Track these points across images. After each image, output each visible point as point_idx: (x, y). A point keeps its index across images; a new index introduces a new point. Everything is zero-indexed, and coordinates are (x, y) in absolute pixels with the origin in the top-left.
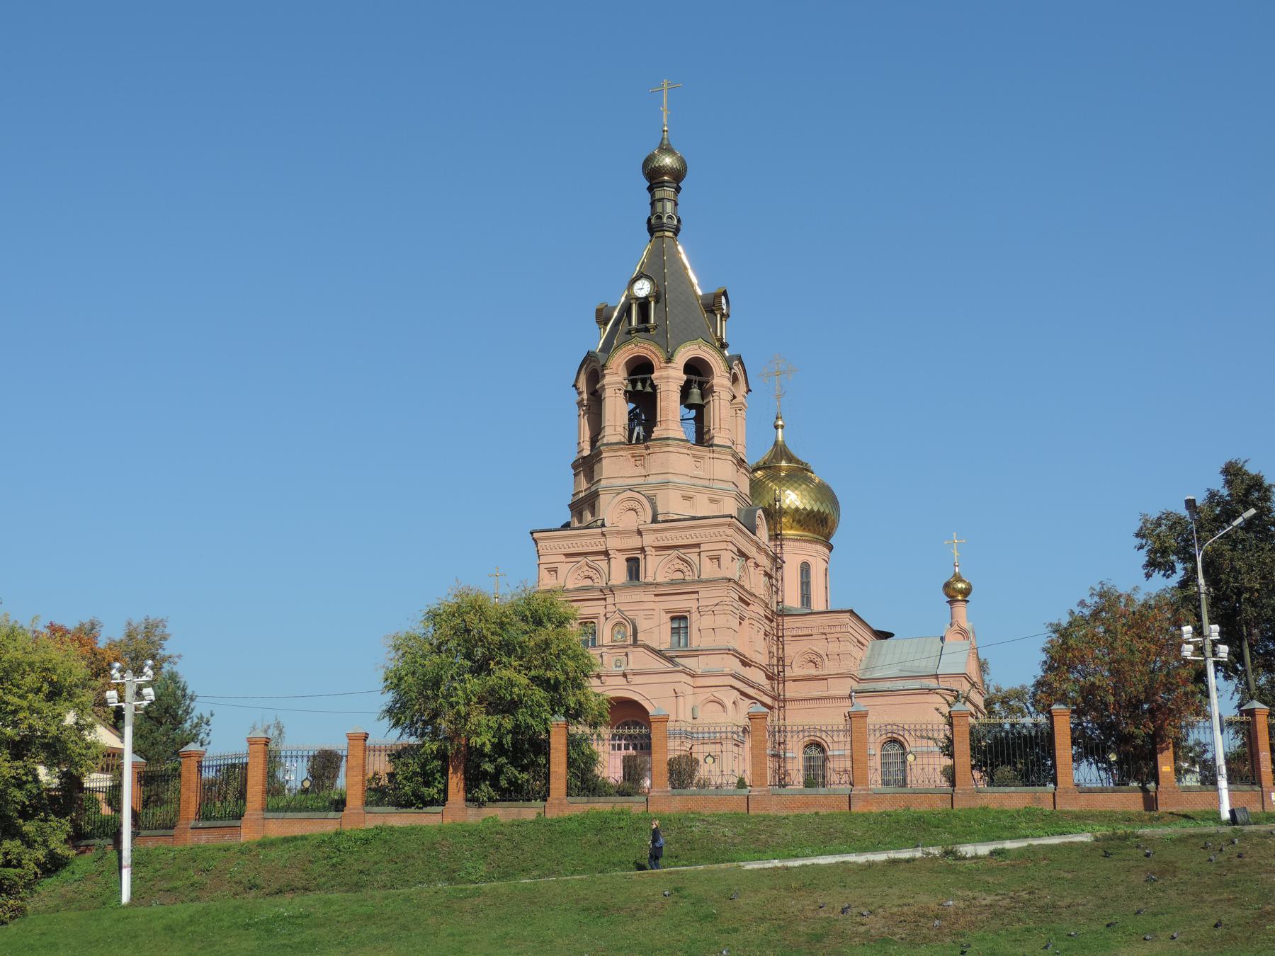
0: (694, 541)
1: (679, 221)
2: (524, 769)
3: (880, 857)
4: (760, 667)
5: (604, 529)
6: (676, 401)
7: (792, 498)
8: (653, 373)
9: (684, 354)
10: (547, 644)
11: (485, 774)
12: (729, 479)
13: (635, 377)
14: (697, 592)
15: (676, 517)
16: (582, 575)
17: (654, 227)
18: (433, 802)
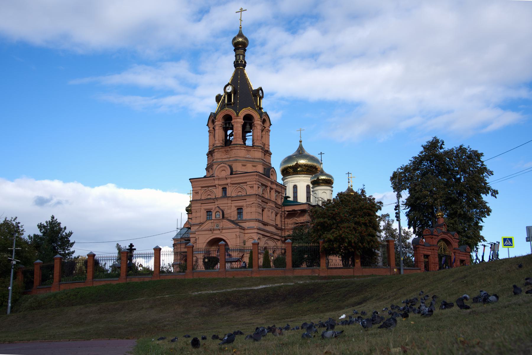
4: (272, 226)
5: (214, 178)
6: (240, 131)
8: (232, 120)
12: (260, 158)
13: (226, 122)
14: (246, 199)
15: (239, 172)
16: (206, 195)
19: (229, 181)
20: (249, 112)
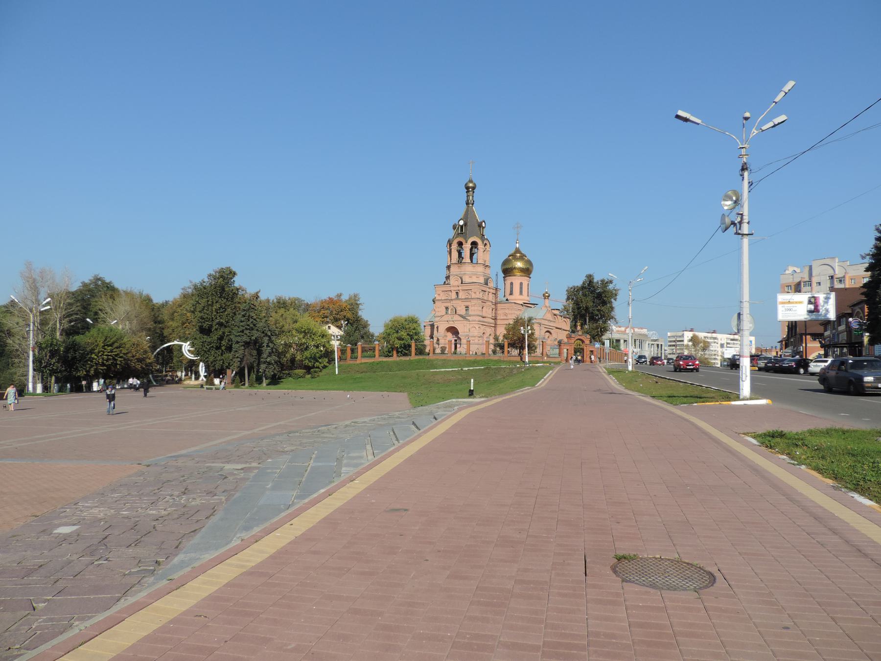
1: (473, 201)
2: (407, 350)
3: (451, 370)
7: (519, 264)
8: (463, 245)
9: (470, 241)
10: (410, 328)
11: (400, 352)
17: (467, 204)
18: (391, 356)
19: (460, 288)
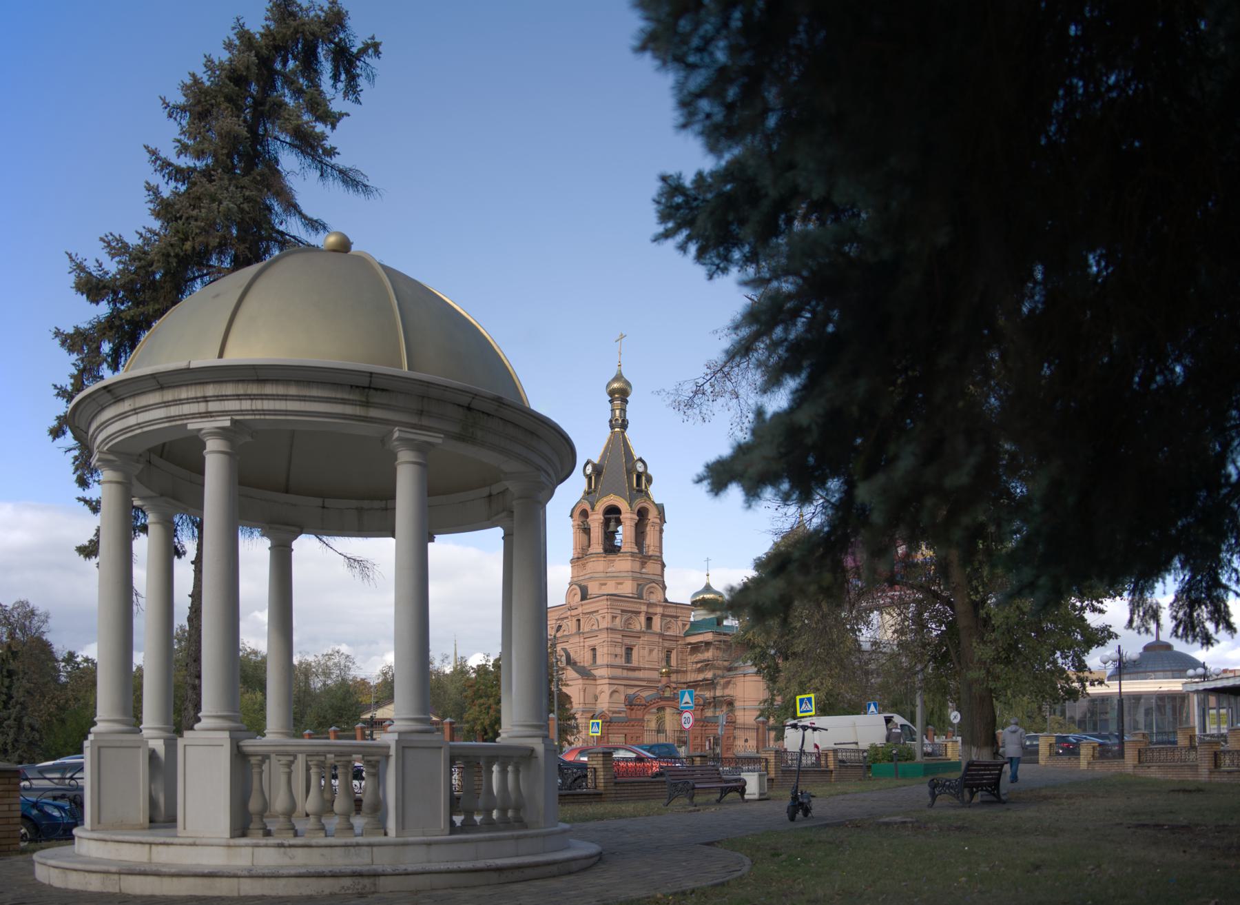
0: (595, 609)
19: (580, 610)
20: (604, 506)
